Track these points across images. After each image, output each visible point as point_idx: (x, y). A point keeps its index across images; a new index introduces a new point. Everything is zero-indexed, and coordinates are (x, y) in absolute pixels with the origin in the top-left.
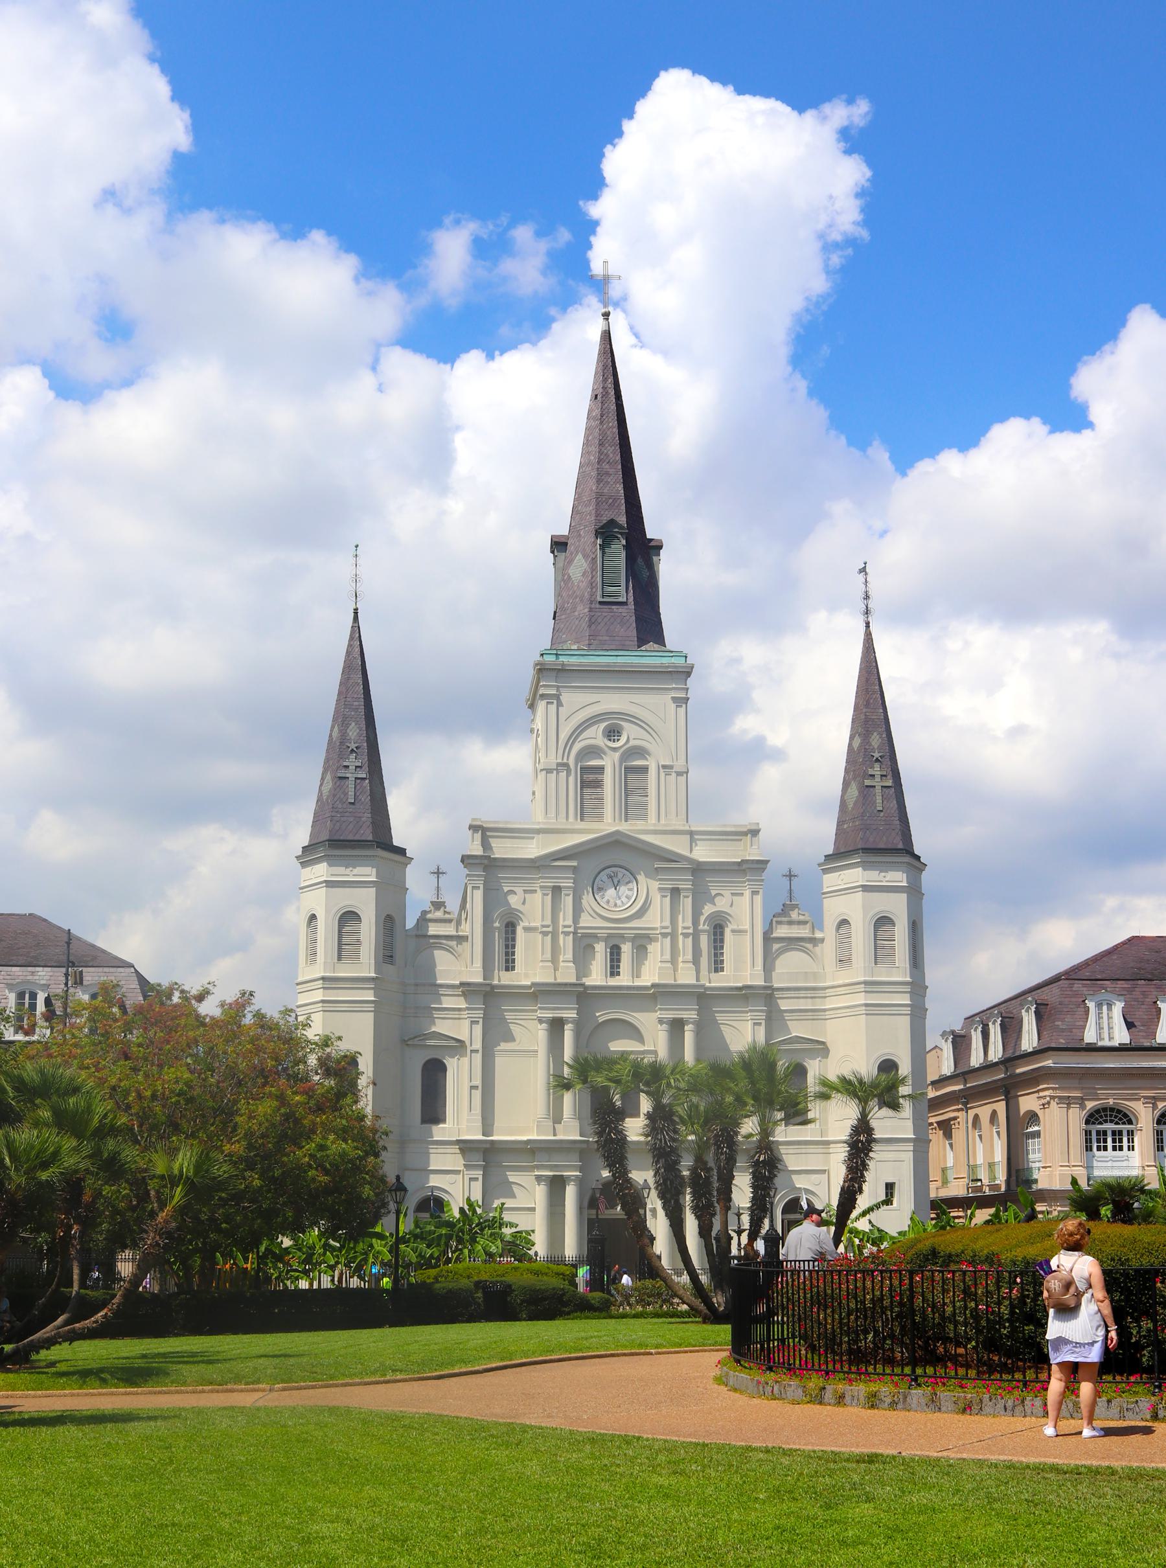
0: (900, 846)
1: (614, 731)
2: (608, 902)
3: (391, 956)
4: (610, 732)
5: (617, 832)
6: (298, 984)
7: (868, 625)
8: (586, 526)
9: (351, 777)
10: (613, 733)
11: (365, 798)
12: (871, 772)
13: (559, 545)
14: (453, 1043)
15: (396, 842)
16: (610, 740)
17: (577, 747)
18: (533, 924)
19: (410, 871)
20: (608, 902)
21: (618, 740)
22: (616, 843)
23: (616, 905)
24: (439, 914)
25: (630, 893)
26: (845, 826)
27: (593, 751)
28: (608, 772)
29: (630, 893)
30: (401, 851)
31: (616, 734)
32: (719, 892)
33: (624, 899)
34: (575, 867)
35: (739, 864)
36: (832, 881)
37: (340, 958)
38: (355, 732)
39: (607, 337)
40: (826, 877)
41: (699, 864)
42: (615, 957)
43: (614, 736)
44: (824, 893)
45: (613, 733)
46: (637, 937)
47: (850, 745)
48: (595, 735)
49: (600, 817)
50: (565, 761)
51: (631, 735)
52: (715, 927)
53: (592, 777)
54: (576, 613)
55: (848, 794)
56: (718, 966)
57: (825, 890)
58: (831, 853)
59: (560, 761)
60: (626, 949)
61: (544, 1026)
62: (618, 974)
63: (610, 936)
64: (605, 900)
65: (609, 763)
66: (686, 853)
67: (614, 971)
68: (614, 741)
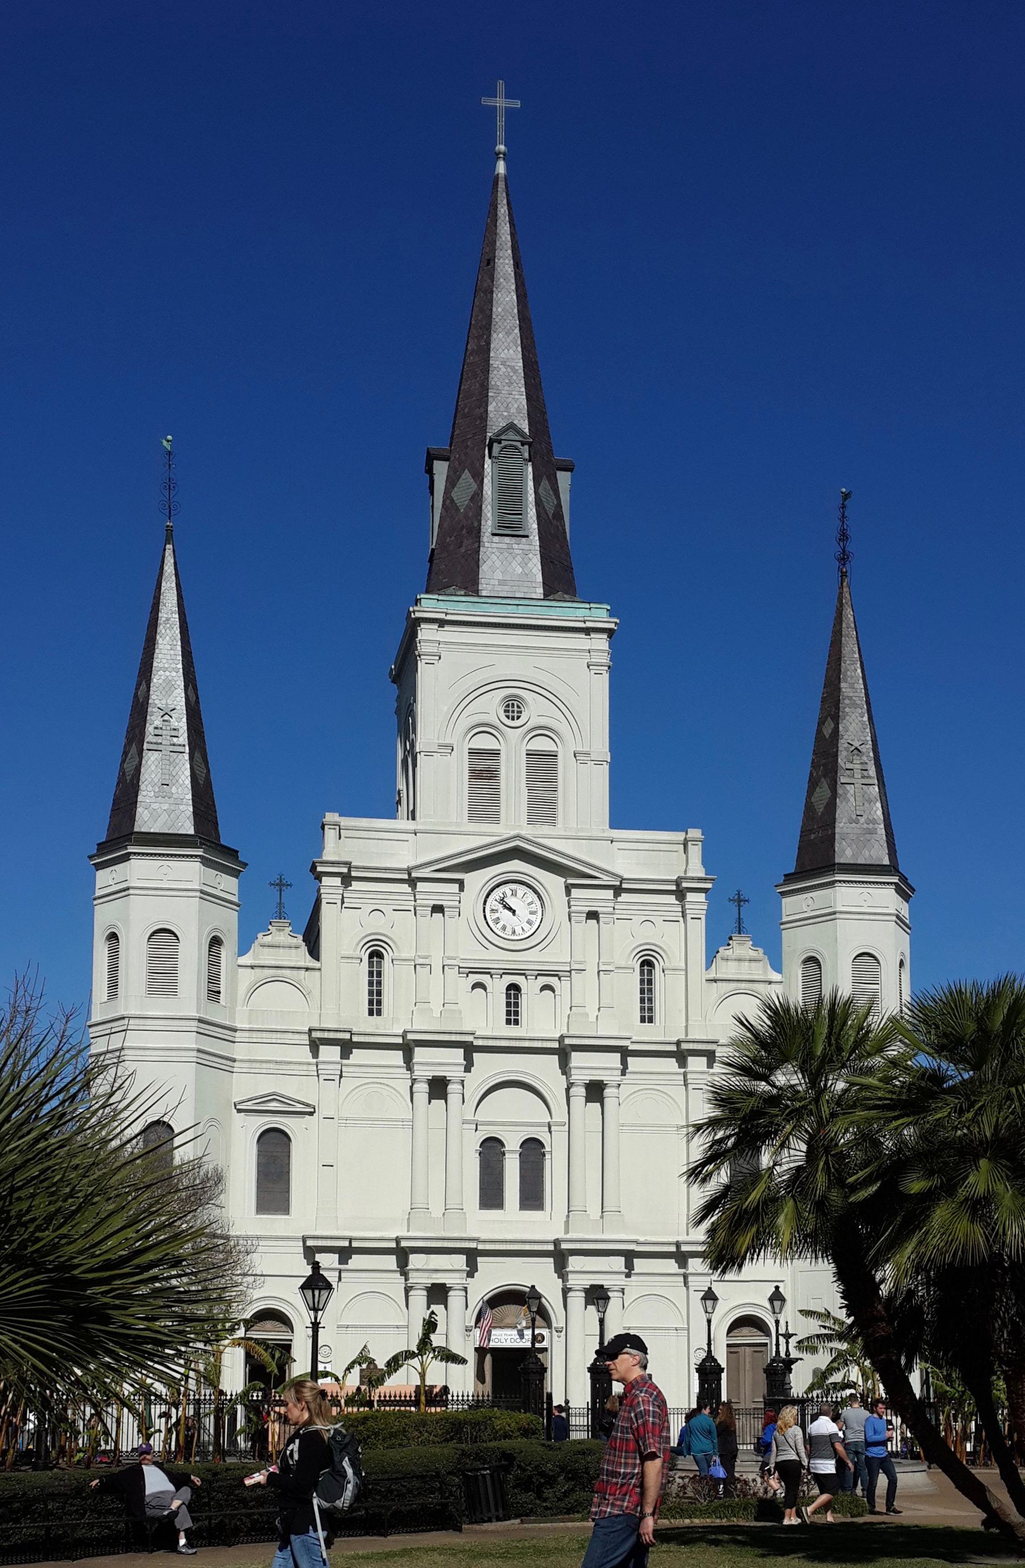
0: (886, 861)
1: (513, 704)
2: (504, 928)
3: (219, 992)
4: (508, 706)
5: (518, 837)
6: (90, 1026)
8: (475, 434)
10: (513, 708)
12: (849, 766)
14: (299, 1108)
16: (508, 717)
17: (465, 723)
18: (404, 955)
20: (504, 928)
21: (518, 718)
23: (514, 932)
25: (533, 918)
26: (813, 836)
27: (483, 728)
29: (533, 918)
31: (516, 709)
32: (647, 918)
33: (526, 927)
35: (678, 882)
36: (793, 906)
40: (784, 900)
41: (623, 880)
42: (512, 1000)
43: (513, 712)
44: (782, 924)
45: (513, 708)
46: (542, 974)
47: (819, 731)
48: (491, 708)
49: (495, 818)
50: (447, 741)
51: (535, 711)
52: (642, 964)
53: (483, 764)
54: (463, 550)
55: (816, 795)
56: (647, 1017)
57: (785, 919)
58: (793, 871)
59: (441, 741)
60: (529, 987)
61: (423, 1088)
62: (516, 1022)
63: (508, 972)
64: (500, 926)
67: (513, 1016)
68: (513, 719)
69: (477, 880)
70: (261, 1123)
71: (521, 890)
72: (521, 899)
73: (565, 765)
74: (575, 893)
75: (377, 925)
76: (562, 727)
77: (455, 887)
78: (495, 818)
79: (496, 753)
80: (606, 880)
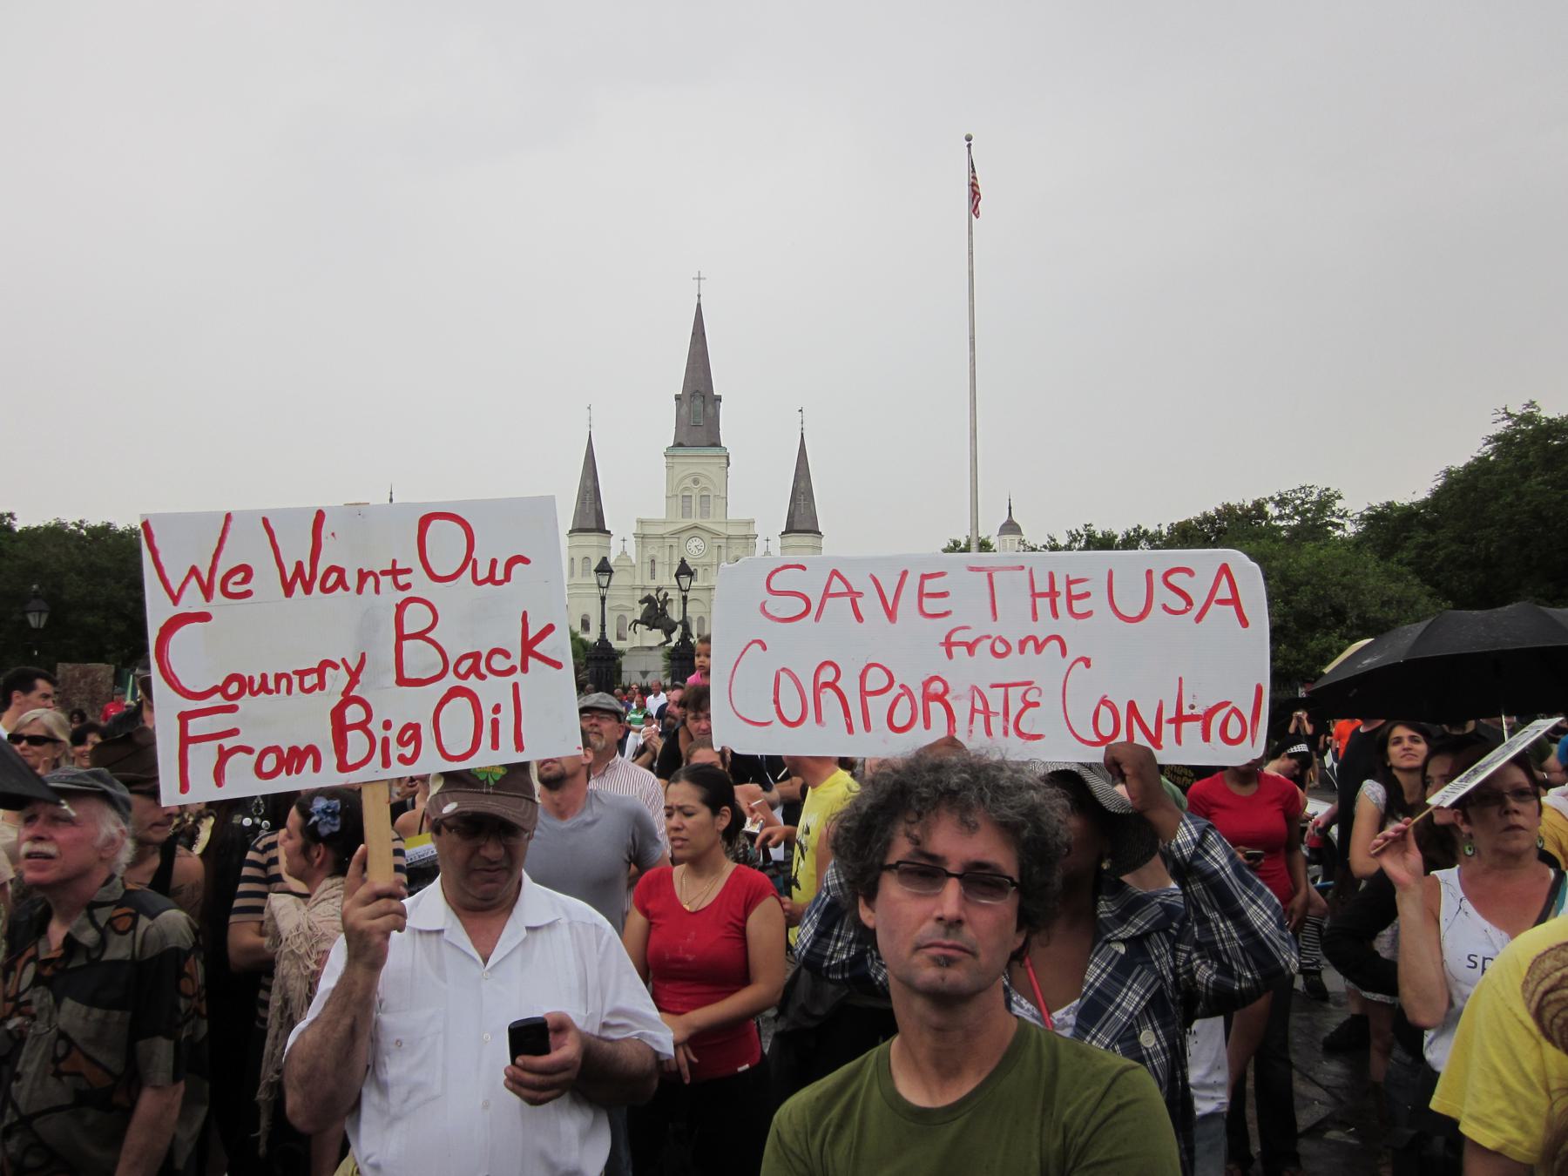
7: (802, 434)
9: (587, 504)
10: (696, 482)
11: (593, 512)
13: (678, 398)
15: (607, 529)
17: (681, 488)
19: (612, 539)
22: (696, 527)
24: (624, 557)
27: (686, 489)
28: (693, 498)
30: (609, 532)
34: (678, 538)
37: (582, 576)
38: (589, 483)
39: (699, 306)
45: (696, 482)
48: (688, 483)
51: (703, 482)
65: (695, 492)
66: (724, 531)
69: (685, 536)
70: (616, 614)
71: (698, 539)
72: (697, 542)
73: (711, 498)
74: (715, 540)
75: (653, 552)
76: (712, 488)
77: (676, 540)
78: (691, 517)
79: (691, 496)
80: (723, 536)
